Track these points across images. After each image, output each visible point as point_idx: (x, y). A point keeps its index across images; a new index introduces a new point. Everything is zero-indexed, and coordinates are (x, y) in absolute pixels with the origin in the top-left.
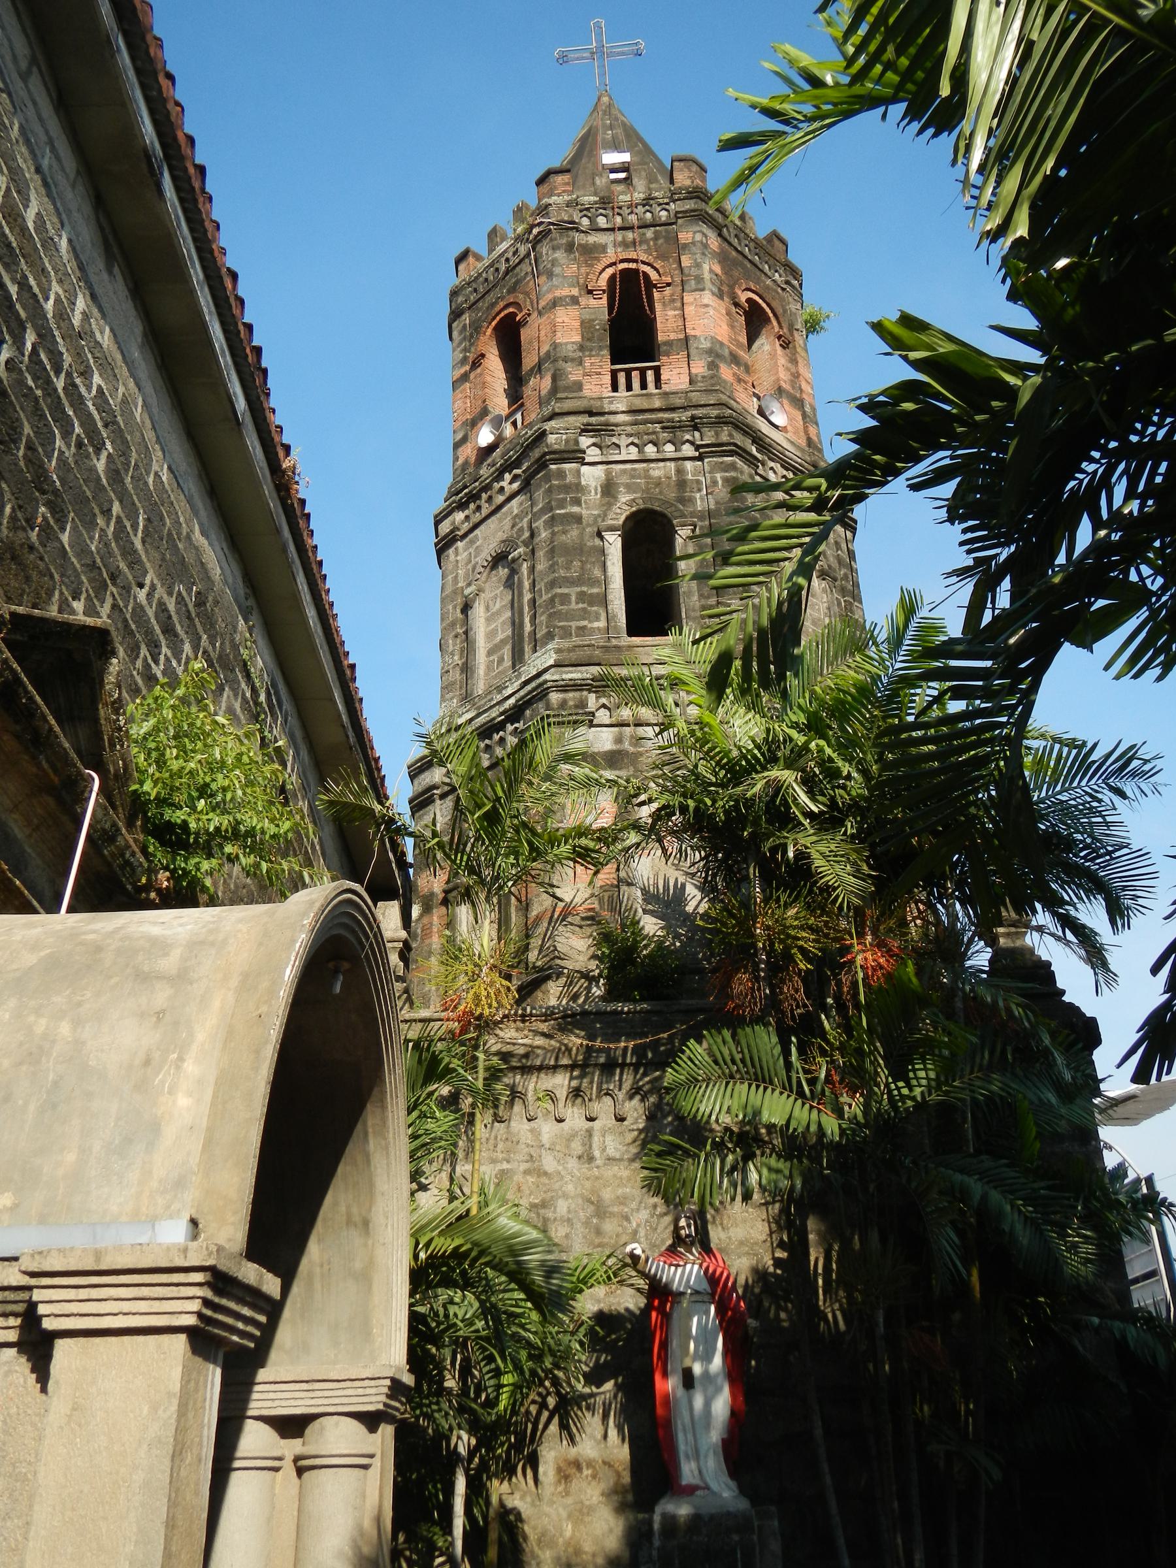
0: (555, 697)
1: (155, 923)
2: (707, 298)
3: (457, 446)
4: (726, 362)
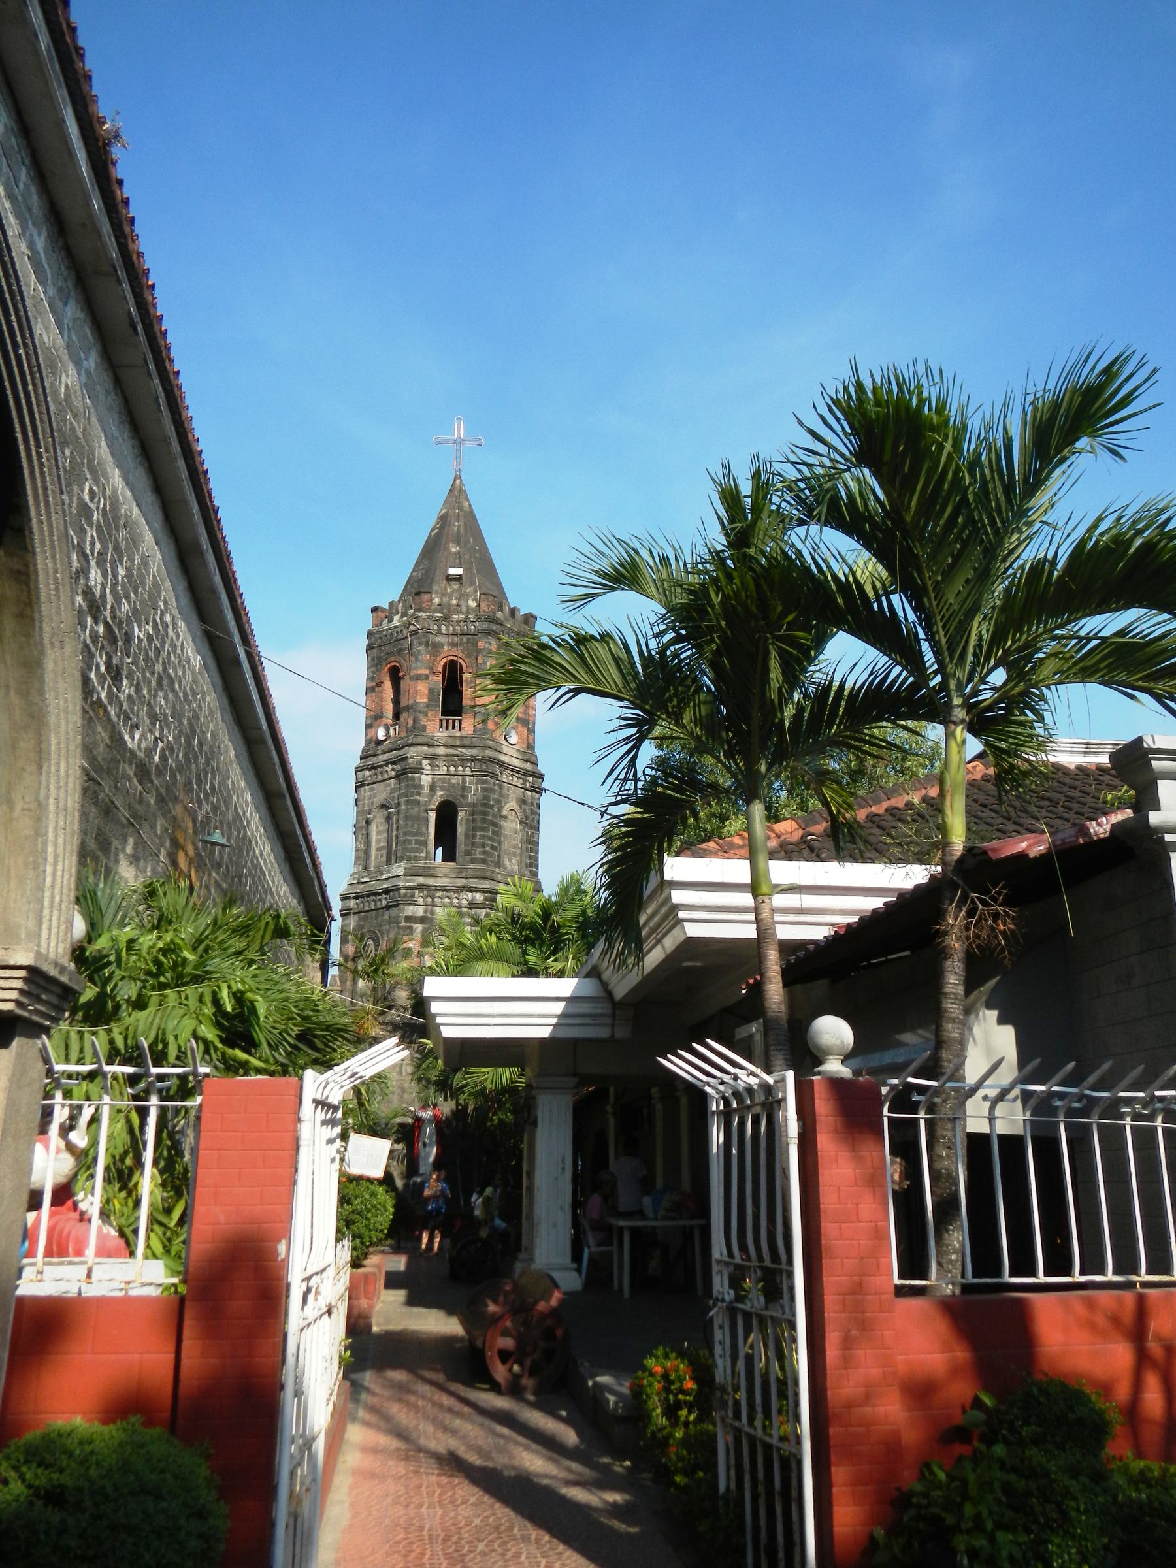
0: (402, 891)
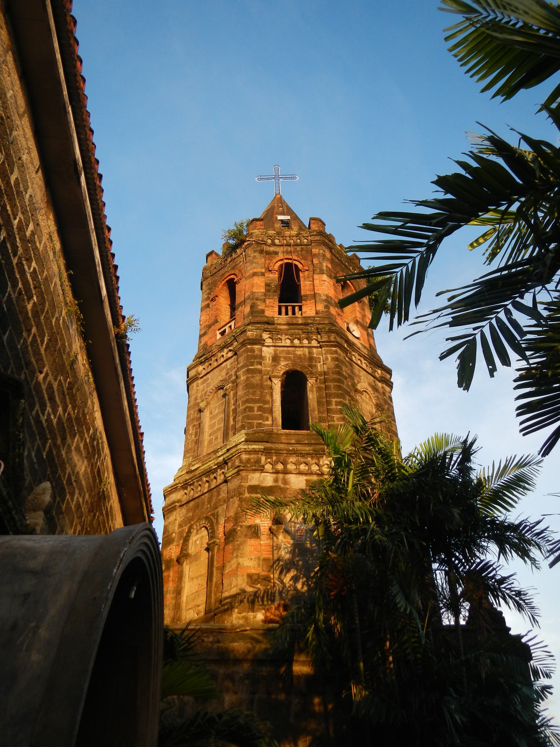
1: (29, 540)
2: (325, 277)
3: (201, 336)
4: (333, 306)
